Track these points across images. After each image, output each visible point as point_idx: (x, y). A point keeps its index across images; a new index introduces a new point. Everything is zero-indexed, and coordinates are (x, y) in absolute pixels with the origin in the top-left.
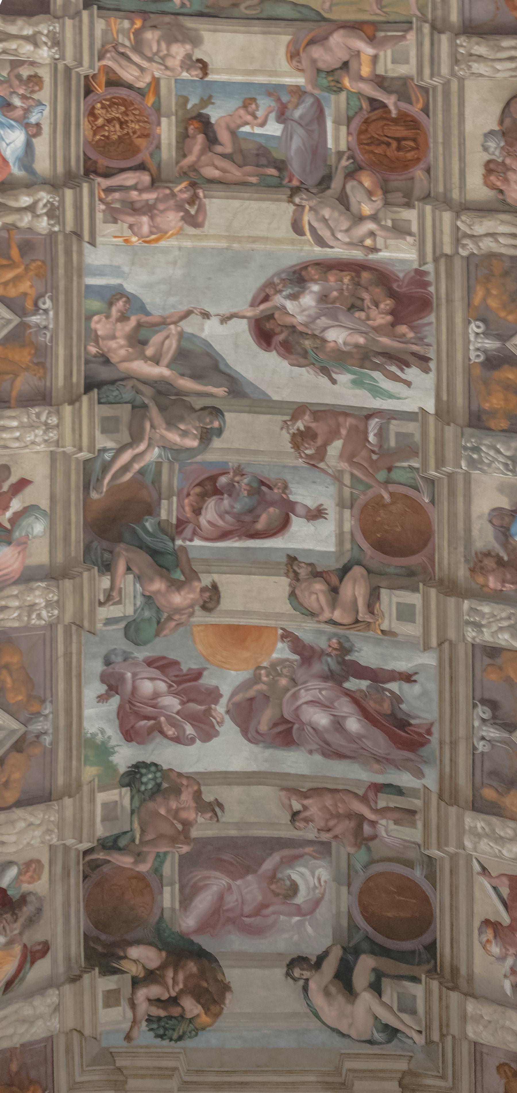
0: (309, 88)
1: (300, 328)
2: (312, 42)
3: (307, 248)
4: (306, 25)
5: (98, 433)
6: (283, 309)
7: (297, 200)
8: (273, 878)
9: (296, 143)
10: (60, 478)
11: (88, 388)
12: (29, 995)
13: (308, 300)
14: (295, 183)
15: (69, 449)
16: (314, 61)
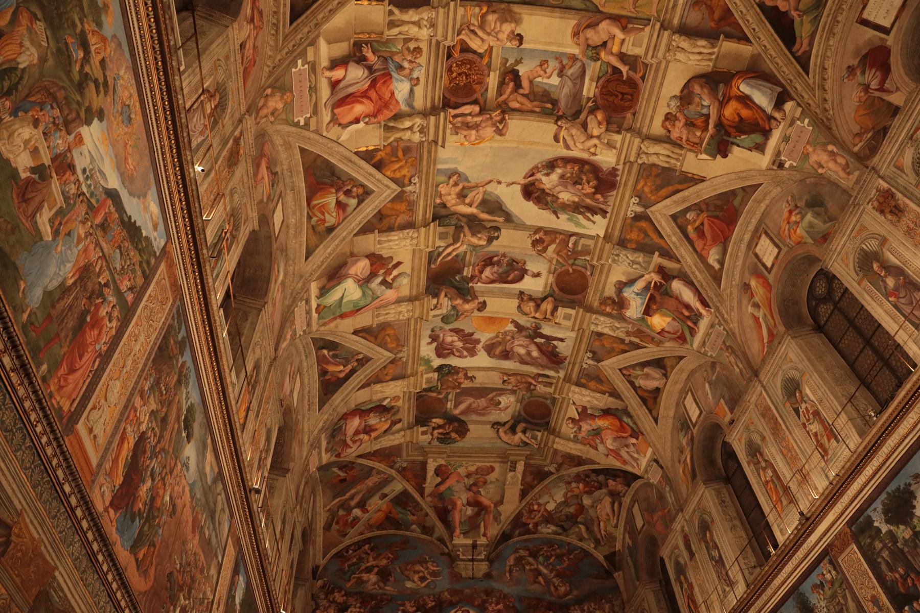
0: (580, 57)
1: (547, 191)
2: (588, 27)
3: (559, 149)
4: (587, 14)
5: (437, 239)
6: (540, 181)
7: (559, 123)
8: (492, 399)
9: (566, 90)
10: (417, 260)
11: (434, 220)
12: (394, 433)
13: (554, 177)
14: (560, 113)
15: (422, 247)
16: (587, 39)
